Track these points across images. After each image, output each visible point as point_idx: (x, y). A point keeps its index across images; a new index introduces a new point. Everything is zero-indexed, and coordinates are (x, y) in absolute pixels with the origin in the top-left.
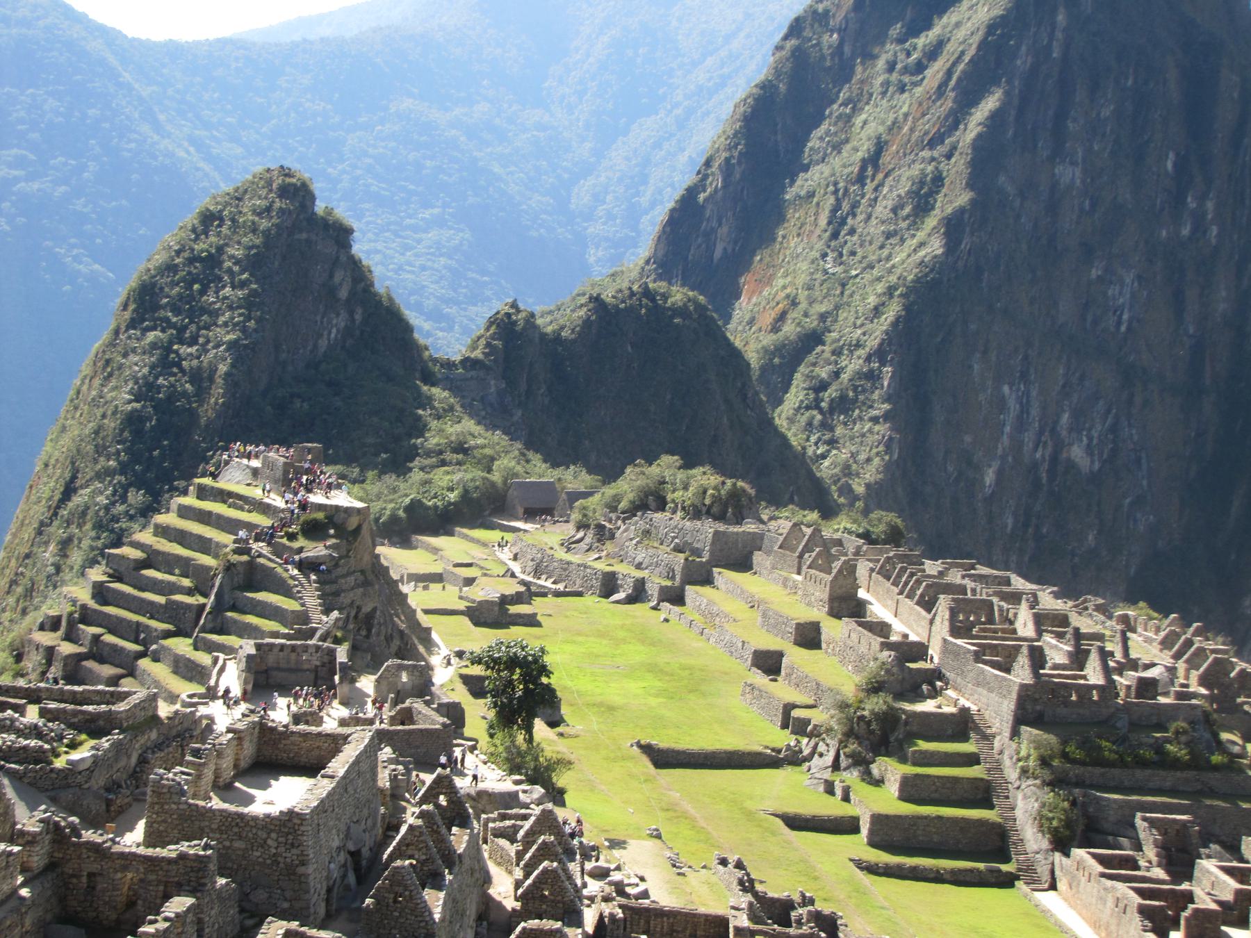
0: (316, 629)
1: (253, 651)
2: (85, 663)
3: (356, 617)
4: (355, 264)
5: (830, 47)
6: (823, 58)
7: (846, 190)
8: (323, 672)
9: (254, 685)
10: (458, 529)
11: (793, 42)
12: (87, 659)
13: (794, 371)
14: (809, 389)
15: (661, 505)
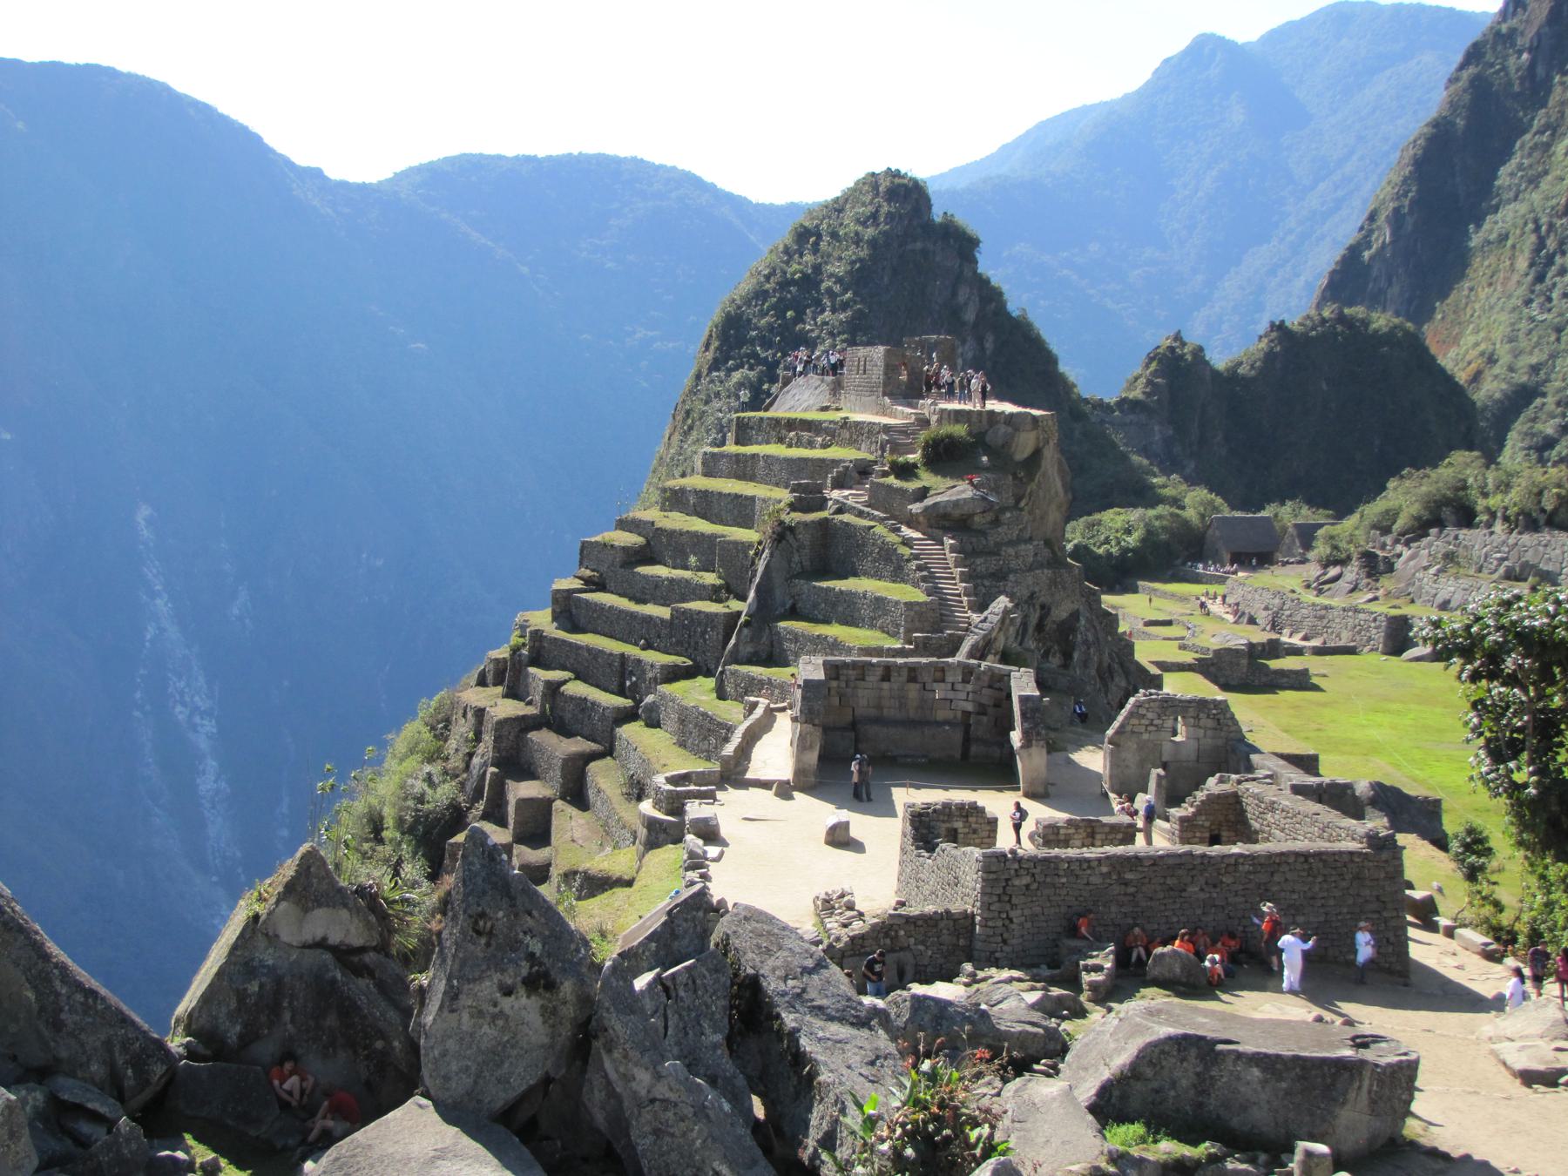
0: (961, 640)
1: (819, 675)
2: (534, 736)
3: (1040, 627)
4: (984, 283)
5: (1518, 70)
6: (1510, 84)
7: (1551, 226)
8: (981, 727)
9: (820, 758)
10: (1140, 583)
11: (1472, 70)
12: (538, 727)
13: (1507, 429)
14: (1529, 448)
15: (1467, 517)
